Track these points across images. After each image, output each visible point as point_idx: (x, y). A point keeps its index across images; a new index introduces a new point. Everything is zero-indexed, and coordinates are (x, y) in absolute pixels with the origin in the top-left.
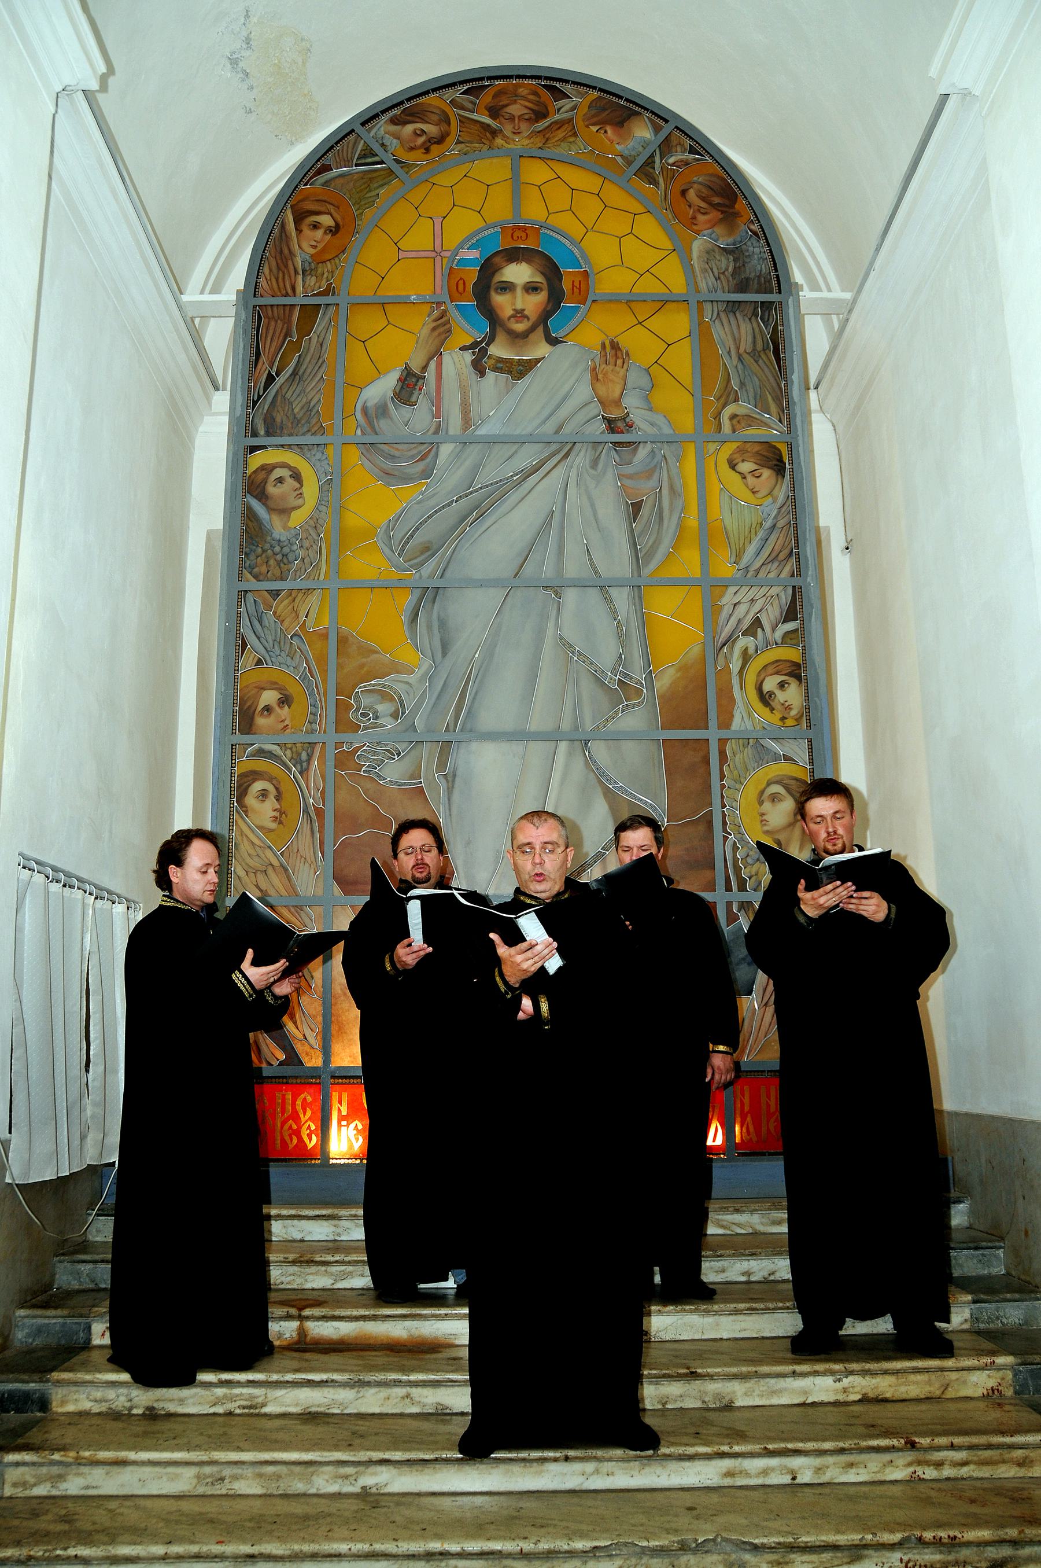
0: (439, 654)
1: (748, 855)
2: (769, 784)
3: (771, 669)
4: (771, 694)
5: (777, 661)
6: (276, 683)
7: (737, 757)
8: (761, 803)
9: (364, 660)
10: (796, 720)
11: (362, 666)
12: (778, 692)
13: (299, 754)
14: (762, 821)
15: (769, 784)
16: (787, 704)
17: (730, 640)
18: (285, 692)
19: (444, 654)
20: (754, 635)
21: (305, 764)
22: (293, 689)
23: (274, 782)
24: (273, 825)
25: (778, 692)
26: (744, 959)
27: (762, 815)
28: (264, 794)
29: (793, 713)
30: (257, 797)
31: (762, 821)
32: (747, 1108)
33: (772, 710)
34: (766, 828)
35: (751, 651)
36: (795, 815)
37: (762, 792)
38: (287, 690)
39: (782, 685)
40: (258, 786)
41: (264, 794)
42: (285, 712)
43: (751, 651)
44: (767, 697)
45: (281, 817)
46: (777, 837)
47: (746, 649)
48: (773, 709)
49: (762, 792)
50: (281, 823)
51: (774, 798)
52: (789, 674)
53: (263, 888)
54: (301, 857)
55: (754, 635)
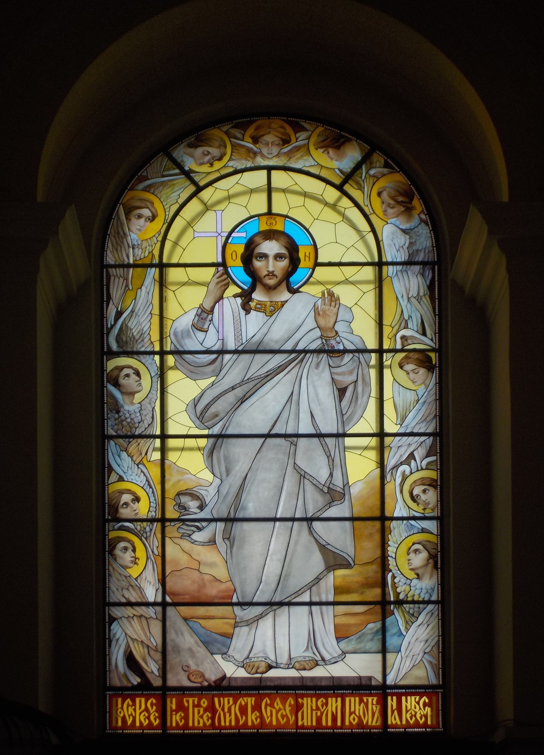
0: (224, 474)
1: (400, 581)
2: (413, 544)
3: (418, 483)
4: (417, 496)
5: (422, 478)
6: (130, 490)
7: (396, 530)
8: (408, 554)
9: (181, 478)
10: (432, 510)
11: (179, 481)
12: (422, 495)
13: (145, 528)
14: (409, 563)
15: (413, 544)
16: (427, 501)
17: (396, 467)
18: (136, 495)
19: (228, 475)
20: (409, 465)
21: (148, 534)
22: (141, 493)
23: (131, 542)
24: (131, 565)
25: (422, 495)
26: (395, 634)
27: (409, 560)
28: (126, 549)
29: (430, 506)
30: (121, 550)
31: (409, 563)
32: (394, 707)
33: (418, 504)
34: (411, 567)
35: (408, 472)
36: (428, 560)
37: (410, 548)
38: (136, 494)
39: (424, 491)
40: (122, 544)
41: (126, 549)
42: (136, 506)
43: (408, 472)
44: (415, 497)
45: (135, 560)
46: (417, 571)
47: (404, 471)
48: (419, 504)
49: (410, 548)
50: (136, 563)
51: (416, 551)
52: (429, 485)
53: (127, 596)
54: (148, 581)
55: (409, 465)
